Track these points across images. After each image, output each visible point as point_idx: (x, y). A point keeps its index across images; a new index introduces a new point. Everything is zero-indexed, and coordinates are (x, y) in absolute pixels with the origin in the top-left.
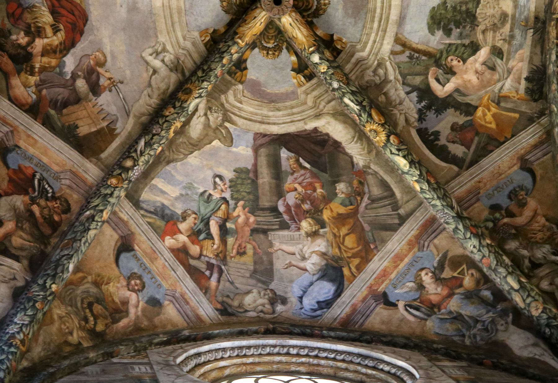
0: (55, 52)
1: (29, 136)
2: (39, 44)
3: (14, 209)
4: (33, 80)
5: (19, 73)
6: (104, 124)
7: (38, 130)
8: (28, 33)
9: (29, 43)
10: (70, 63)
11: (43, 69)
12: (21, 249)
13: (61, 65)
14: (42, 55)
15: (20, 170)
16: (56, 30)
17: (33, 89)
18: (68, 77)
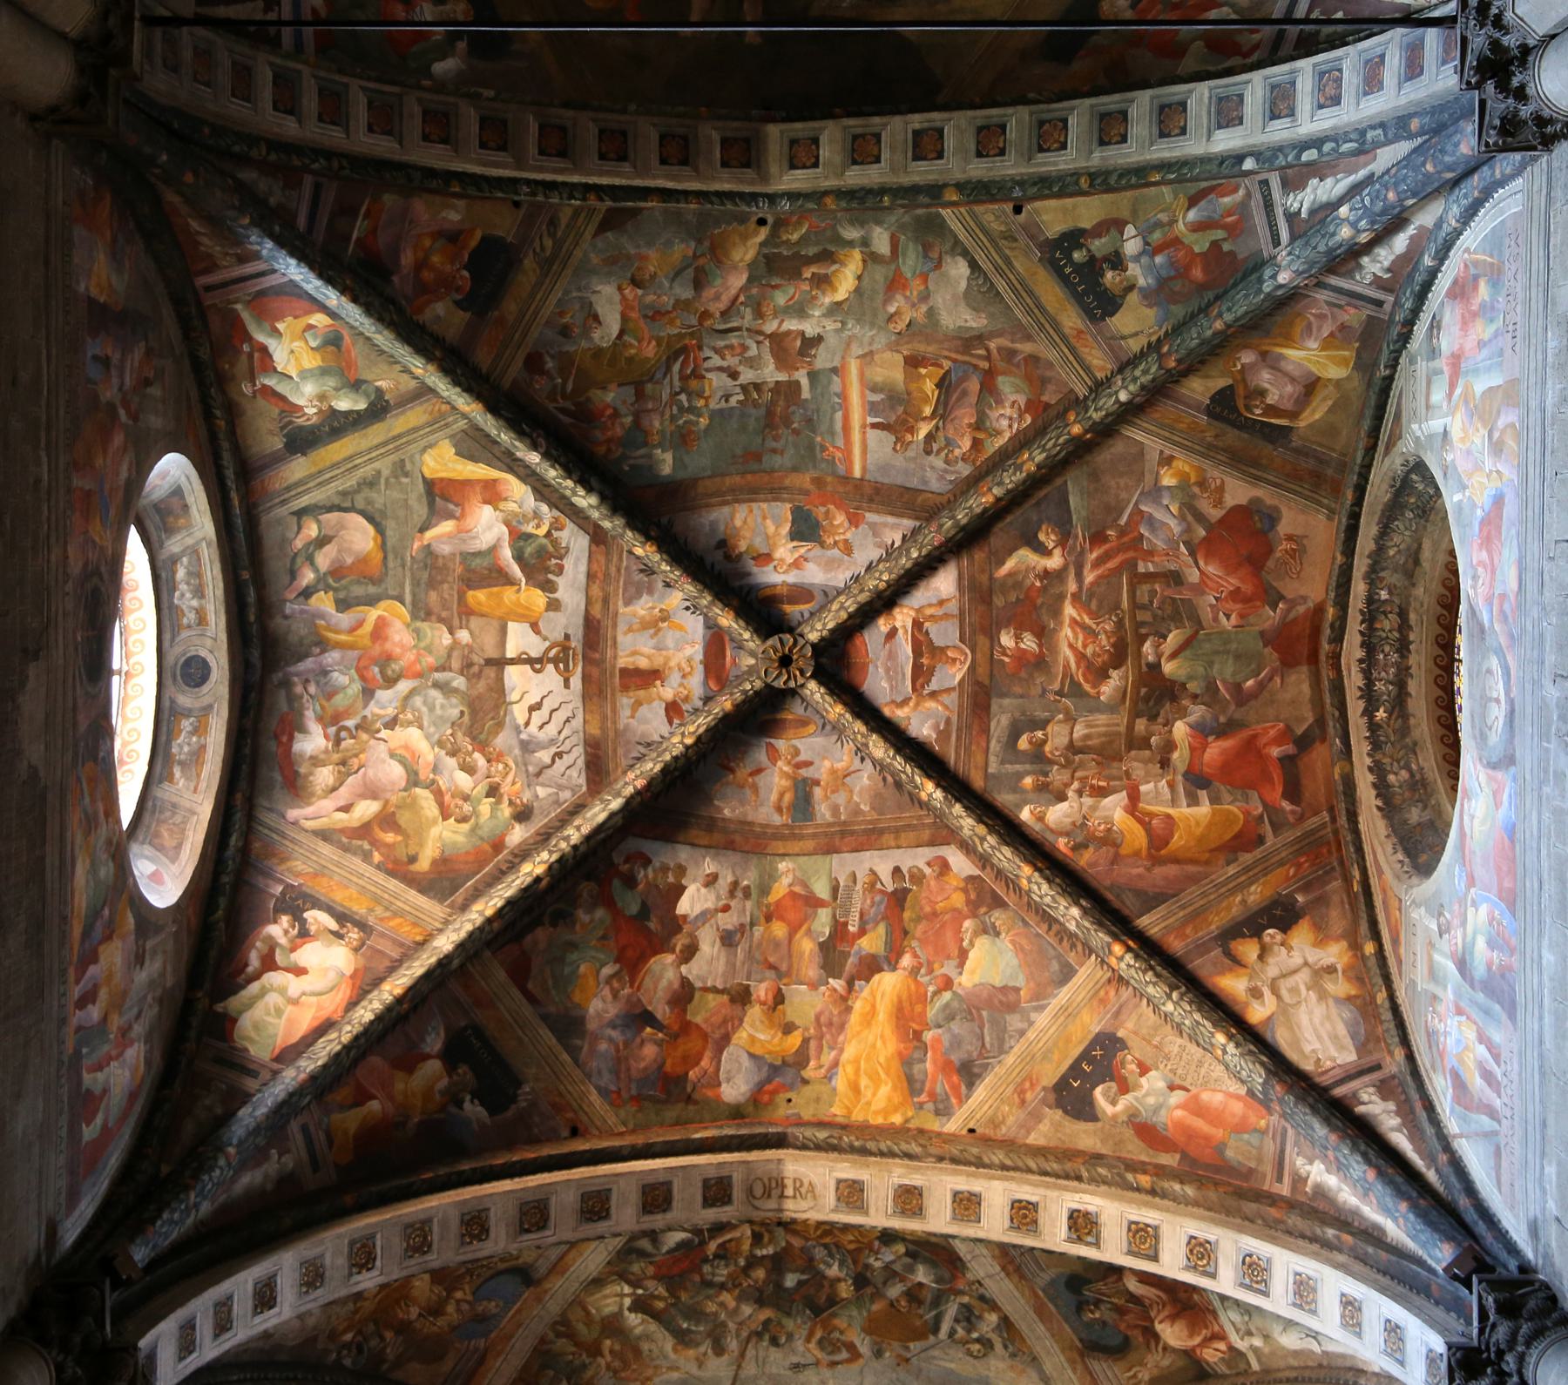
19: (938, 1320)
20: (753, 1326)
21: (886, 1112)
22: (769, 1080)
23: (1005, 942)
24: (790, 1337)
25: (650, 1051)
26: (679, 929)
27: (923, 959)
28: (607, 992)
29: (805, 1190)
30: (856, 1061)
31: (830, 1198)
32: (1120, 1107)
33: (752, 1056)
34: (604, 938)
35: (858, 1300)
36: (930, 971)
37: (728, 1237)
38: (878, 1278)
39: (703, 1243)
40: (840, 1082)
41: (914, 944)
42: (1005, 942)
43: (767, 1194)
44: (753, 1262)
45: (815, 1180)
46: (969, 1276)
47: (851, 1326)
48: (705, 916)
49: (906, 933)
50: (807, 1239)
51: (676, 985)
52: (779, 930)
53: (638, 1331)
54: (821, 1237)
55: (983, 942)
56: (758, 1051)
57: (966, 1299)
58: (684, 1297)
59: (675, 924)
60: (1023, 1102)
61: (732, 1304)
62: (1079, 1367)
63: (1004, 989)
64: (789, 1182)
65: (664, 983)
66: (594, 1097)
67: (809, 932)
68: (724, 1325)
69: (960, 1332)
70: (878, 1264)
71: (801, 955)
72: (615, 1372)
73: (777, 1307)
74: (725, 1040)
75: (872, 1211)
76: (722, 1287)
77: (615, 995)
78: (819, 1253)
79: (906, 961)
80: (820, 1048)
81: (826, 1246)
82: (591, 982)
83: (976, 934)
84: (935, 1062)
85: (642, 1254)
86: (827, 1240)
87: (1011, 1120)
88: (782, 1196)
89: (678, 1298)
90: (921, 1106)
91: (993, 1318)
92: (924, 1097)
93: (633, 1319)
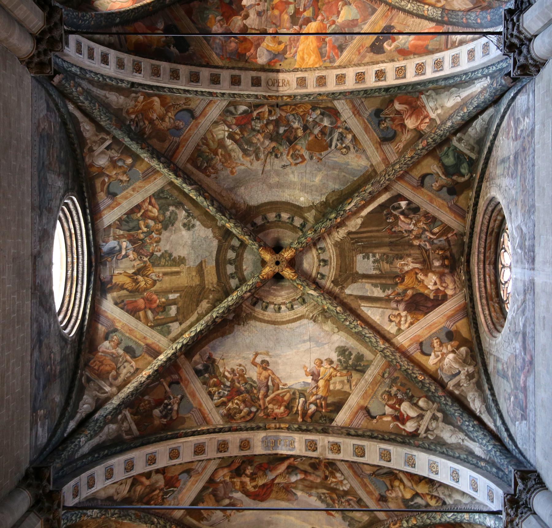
0: (243, 487)
1: (197, 481)
2: (247, 480)
3: (157, 482)
4: (227, 479)
5: (231, 472)
6: (205, 515)
7: (200, 485)
8: (252, 474)
9: (247, 475)
10: (238, 495)
11: (233, 483)
12: (135, 491)
13: (236, 491)
14: (241, 482)
15: (178, 480)
16: (255, 487)
17: (222, 479)
18: (230, 495)
19: (331, 141)
20: (269, 150)
21: (313, 64)
22: (274, 59)
23: (353, 6)
24: (282, 154)
25: (233, 45)
26: (243, 9)
27: (325, 16)
28: (218, 24)
29: (286, 83)
30: (303, 50)
31: (294, 85)
32: (392, 47)
33: (267, 50)
34: (217, 8)
35: (304, 136)
36: (328, 20)
37: (260, 111)
38: (310, 125)
39: (252, 112)
40: (298, 57)
41: (322, 12)
42: (353, 6)
43: (273, 85)
44: (269, 122)
45: (289, 79)
46: (342, 119)
47: (302, 147)
48: (251, 6)
49: (319, 9)
50: (287, 113)
51: (242, 26)
52: (276, 12)
53: (230, 147)
54: (292, 111)
55: (345, 8)
56: (270, 50)
57: (340, 130)
58: (246, 134)
59: (242, 8)
60: (360, 53)
61: (262, 140)
62: (379, 150)
63: (353, 20)
64: (280, 81)
65: (237, 25)
66: (214, 55)
67: (287, 13)
68: (259, 148)
69: (339, 145)
70: (311, 120)
71: (284, 20)
72: (223, 163)
73: (277, 141)
74: (258, 45)
75: (309, 87)
76: (258, 131)
77: (221, 26)
78: (291, 118)
79: (320, 18)
80: (291, 48)
81: (293, 115)
82: (213, 21)
83: (343, 6)
84: (329, 47)
85: (232, 113)
86: (294, 112)
87: (355, 60)
88: (278, 86)
89: (243, 135)
90: (325, 61)
91: (350, 136)
92: (326, 58)
93: (229, 142)
